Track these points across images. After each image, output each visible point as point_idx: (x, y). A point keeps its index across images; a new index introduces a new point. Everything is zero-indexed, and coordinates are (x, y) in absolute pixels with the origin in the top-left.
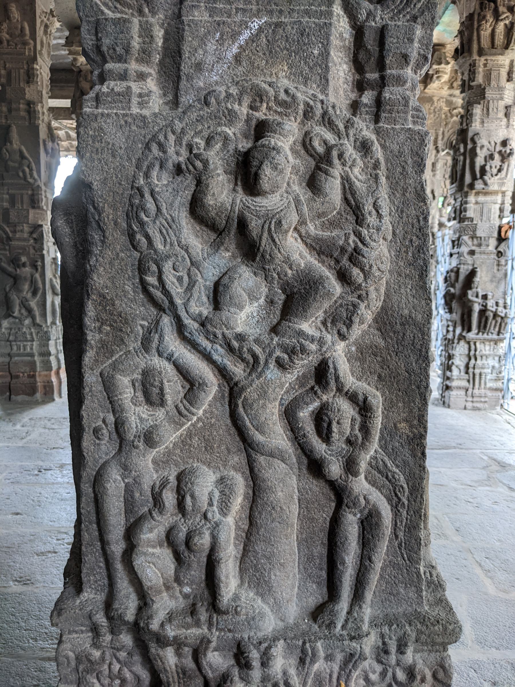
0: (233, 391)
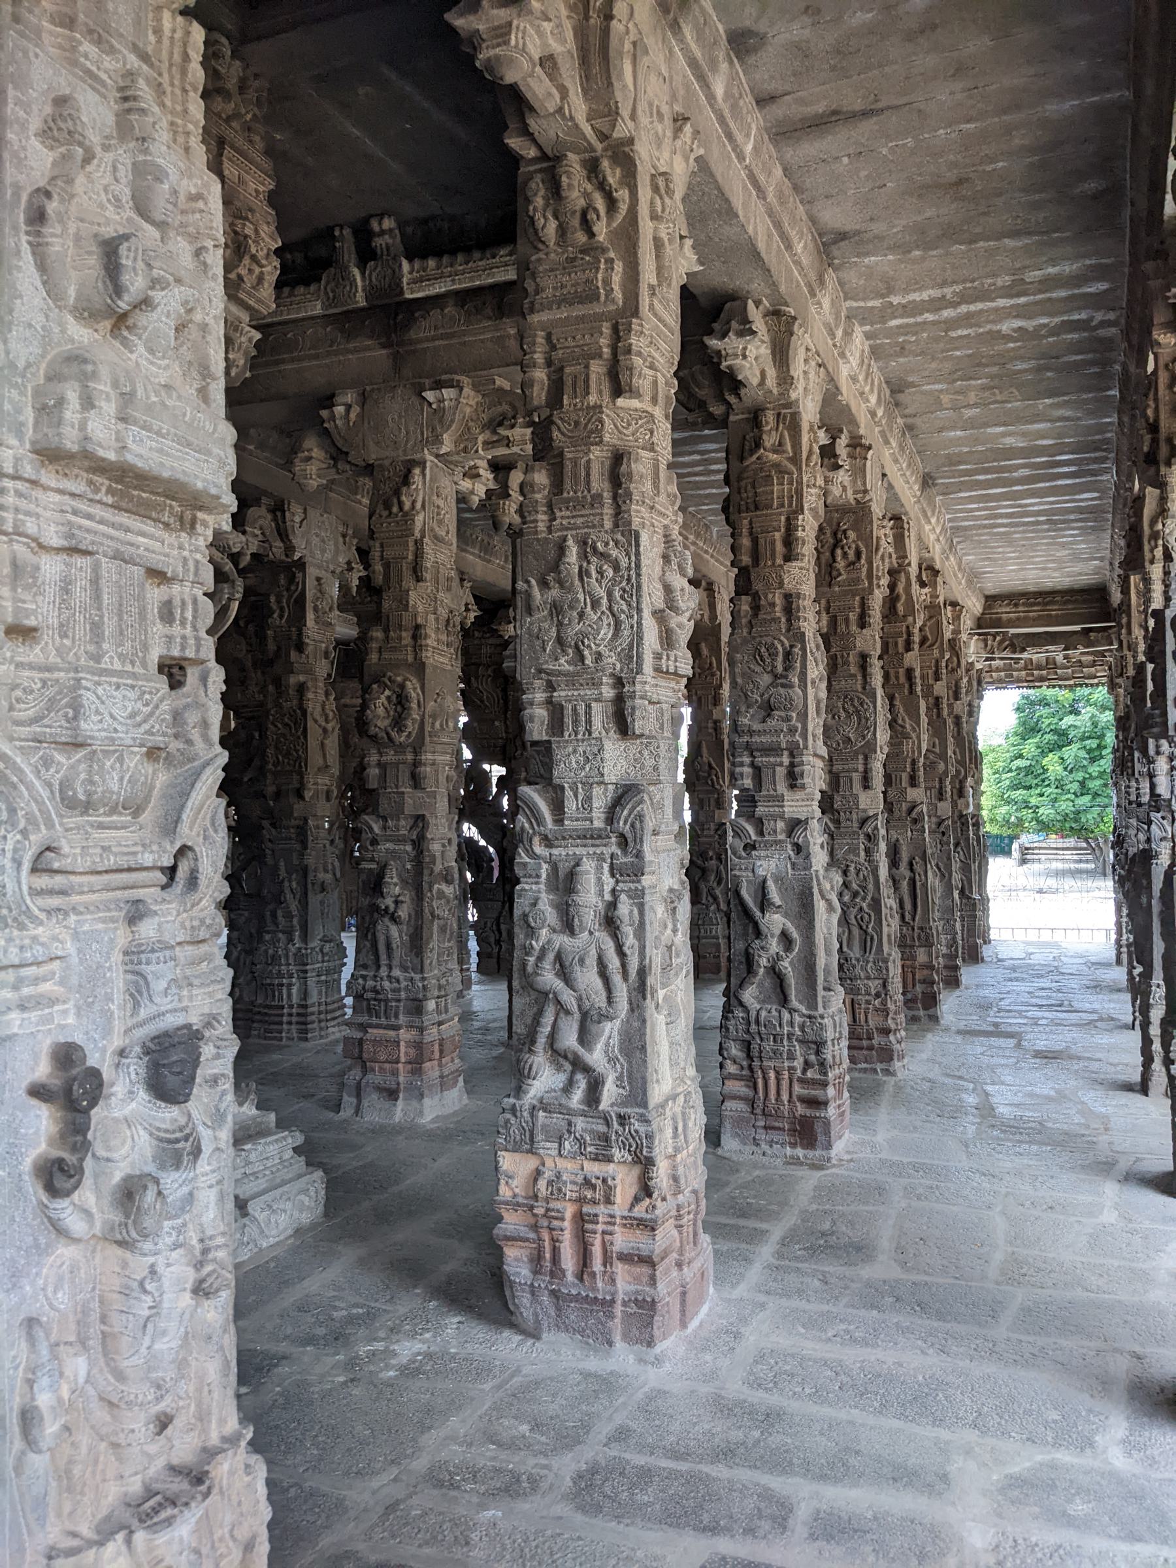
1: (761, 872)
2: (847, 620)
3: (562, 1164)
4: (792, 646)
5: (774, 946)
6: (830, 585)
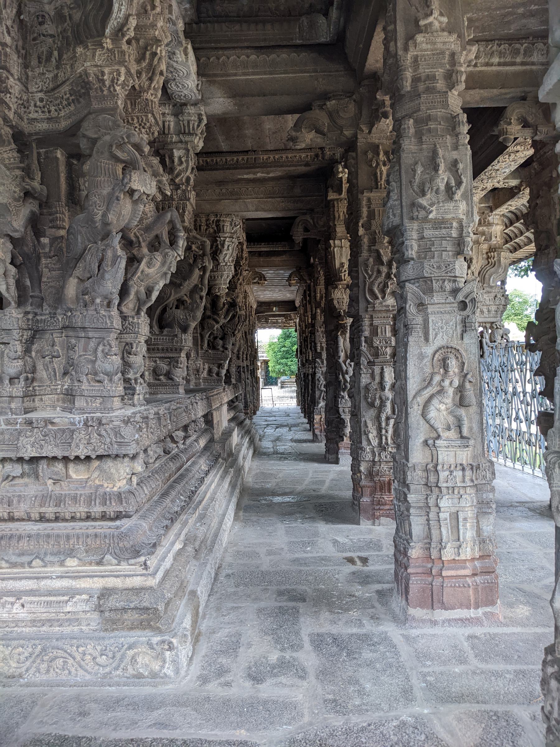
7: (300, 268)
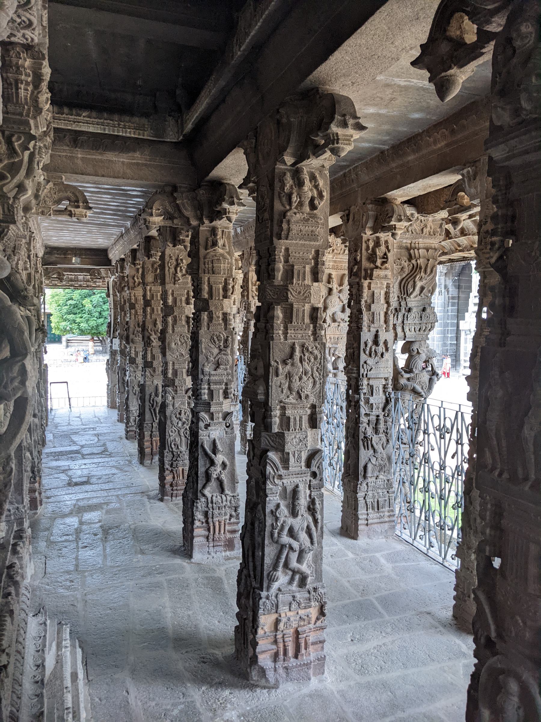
0: (179, 431)
1: (212, 436)
2: (181, 300)
3: (289, 614)
4: (227, 337)
5: (219, 469)
6: (174, 284)
7: (175, 189)
